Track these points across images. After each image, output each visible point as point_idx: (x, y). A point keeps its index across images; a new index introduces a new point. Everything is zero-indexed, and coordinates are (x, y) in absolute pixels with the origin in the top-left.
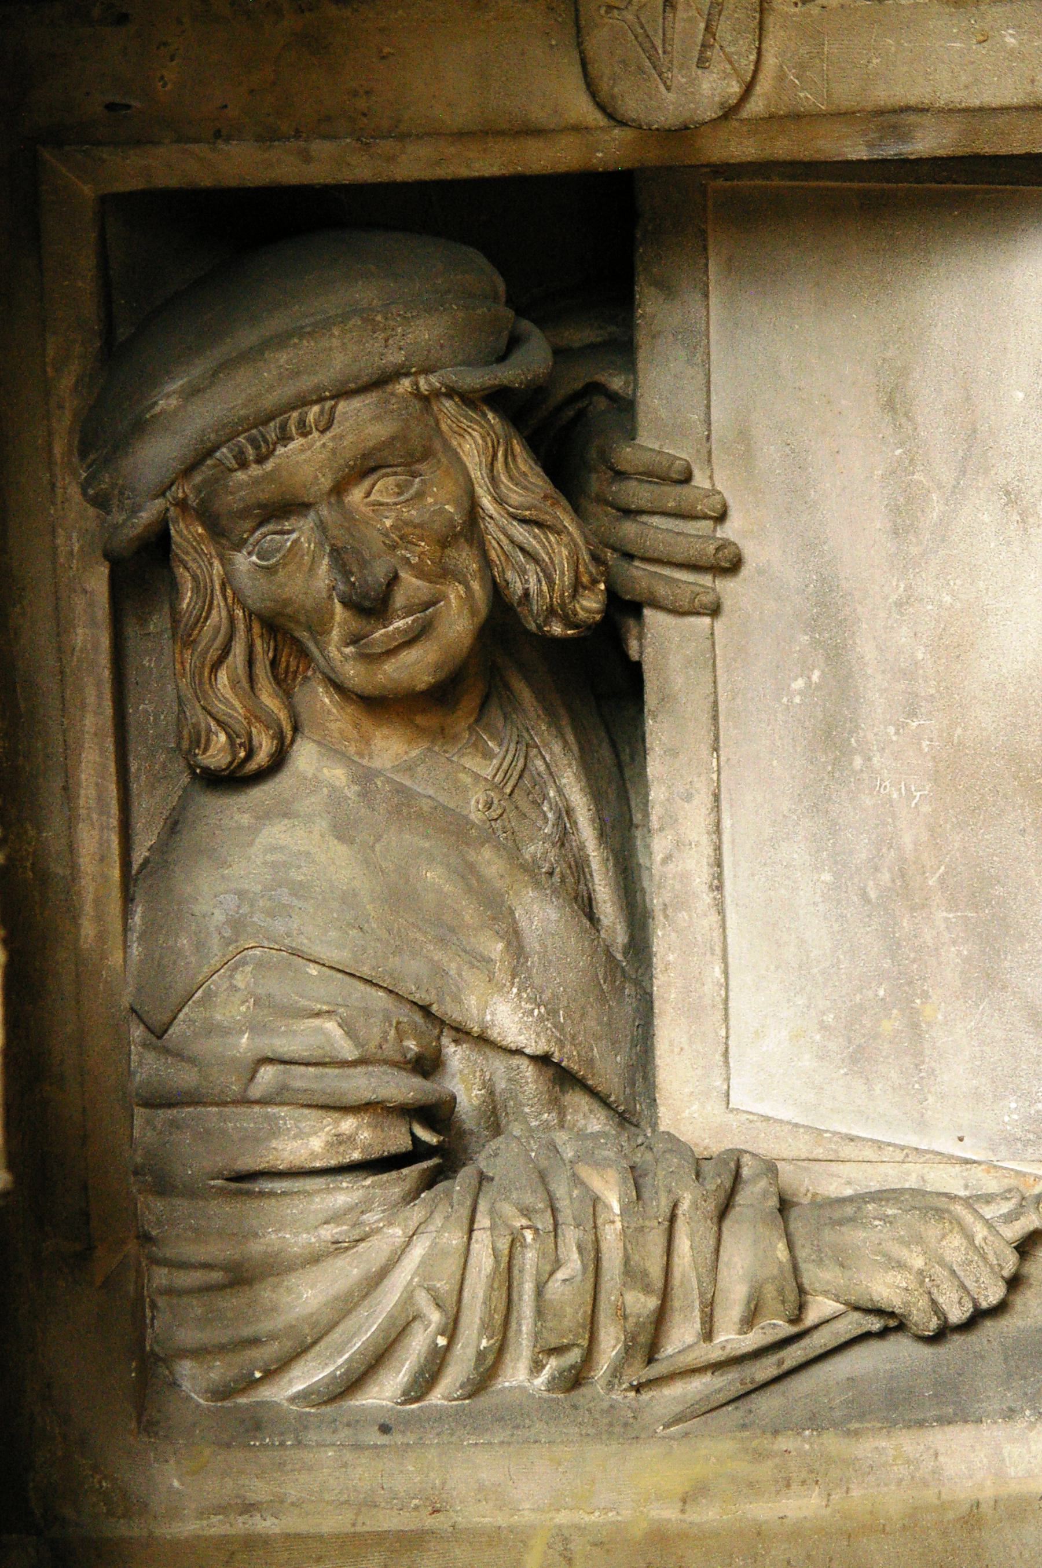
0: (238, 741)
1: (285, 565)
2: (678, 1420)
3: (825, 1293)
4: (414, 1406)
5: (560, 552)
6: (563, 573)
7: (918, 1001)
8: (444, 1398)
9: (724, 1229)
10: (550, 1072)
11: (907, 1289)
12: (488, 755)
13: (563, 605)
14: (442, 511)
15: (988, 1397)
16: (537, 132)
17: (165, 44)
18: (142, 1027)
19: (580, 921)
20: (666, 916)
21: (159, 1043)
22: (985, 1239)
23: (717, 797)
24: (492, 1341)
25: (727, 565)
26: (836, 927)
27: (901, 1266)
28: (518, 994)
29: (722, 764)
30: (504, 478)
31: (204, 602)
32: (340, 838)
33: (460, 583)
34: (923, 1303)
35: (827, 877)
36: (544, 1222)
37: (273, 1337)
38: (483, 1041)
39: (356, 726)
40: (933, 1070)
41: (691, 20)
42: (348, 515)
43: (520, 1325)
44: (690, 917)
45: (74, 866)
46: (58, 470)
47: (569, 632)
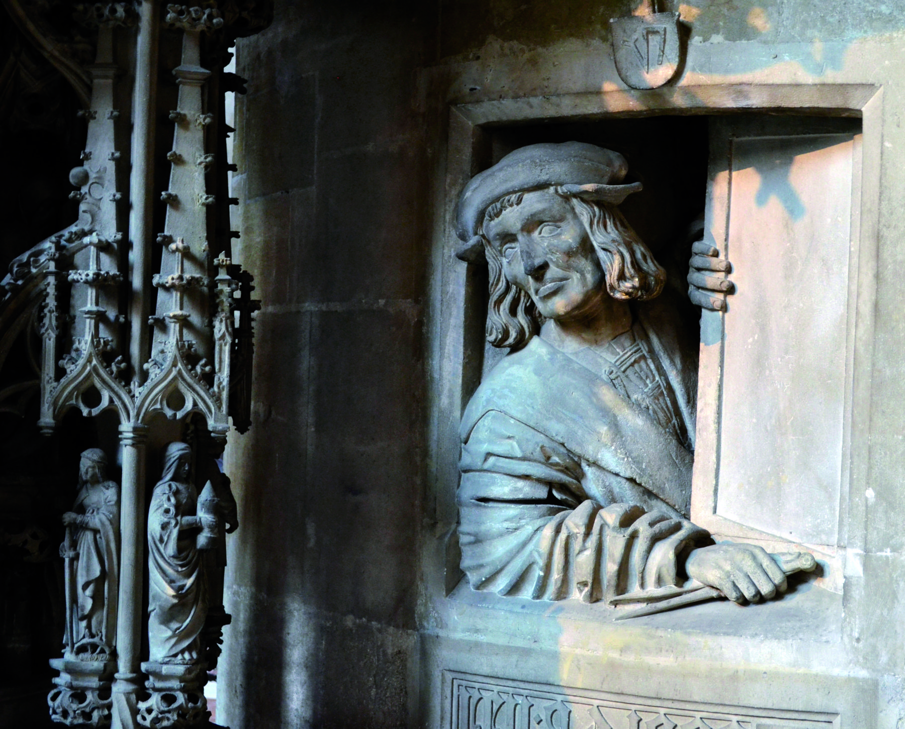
1: (513, 261)
17: (489, 66)
32: (536, 374)
33: (577, 272)
39: (559, 335)
46: (447, 225)
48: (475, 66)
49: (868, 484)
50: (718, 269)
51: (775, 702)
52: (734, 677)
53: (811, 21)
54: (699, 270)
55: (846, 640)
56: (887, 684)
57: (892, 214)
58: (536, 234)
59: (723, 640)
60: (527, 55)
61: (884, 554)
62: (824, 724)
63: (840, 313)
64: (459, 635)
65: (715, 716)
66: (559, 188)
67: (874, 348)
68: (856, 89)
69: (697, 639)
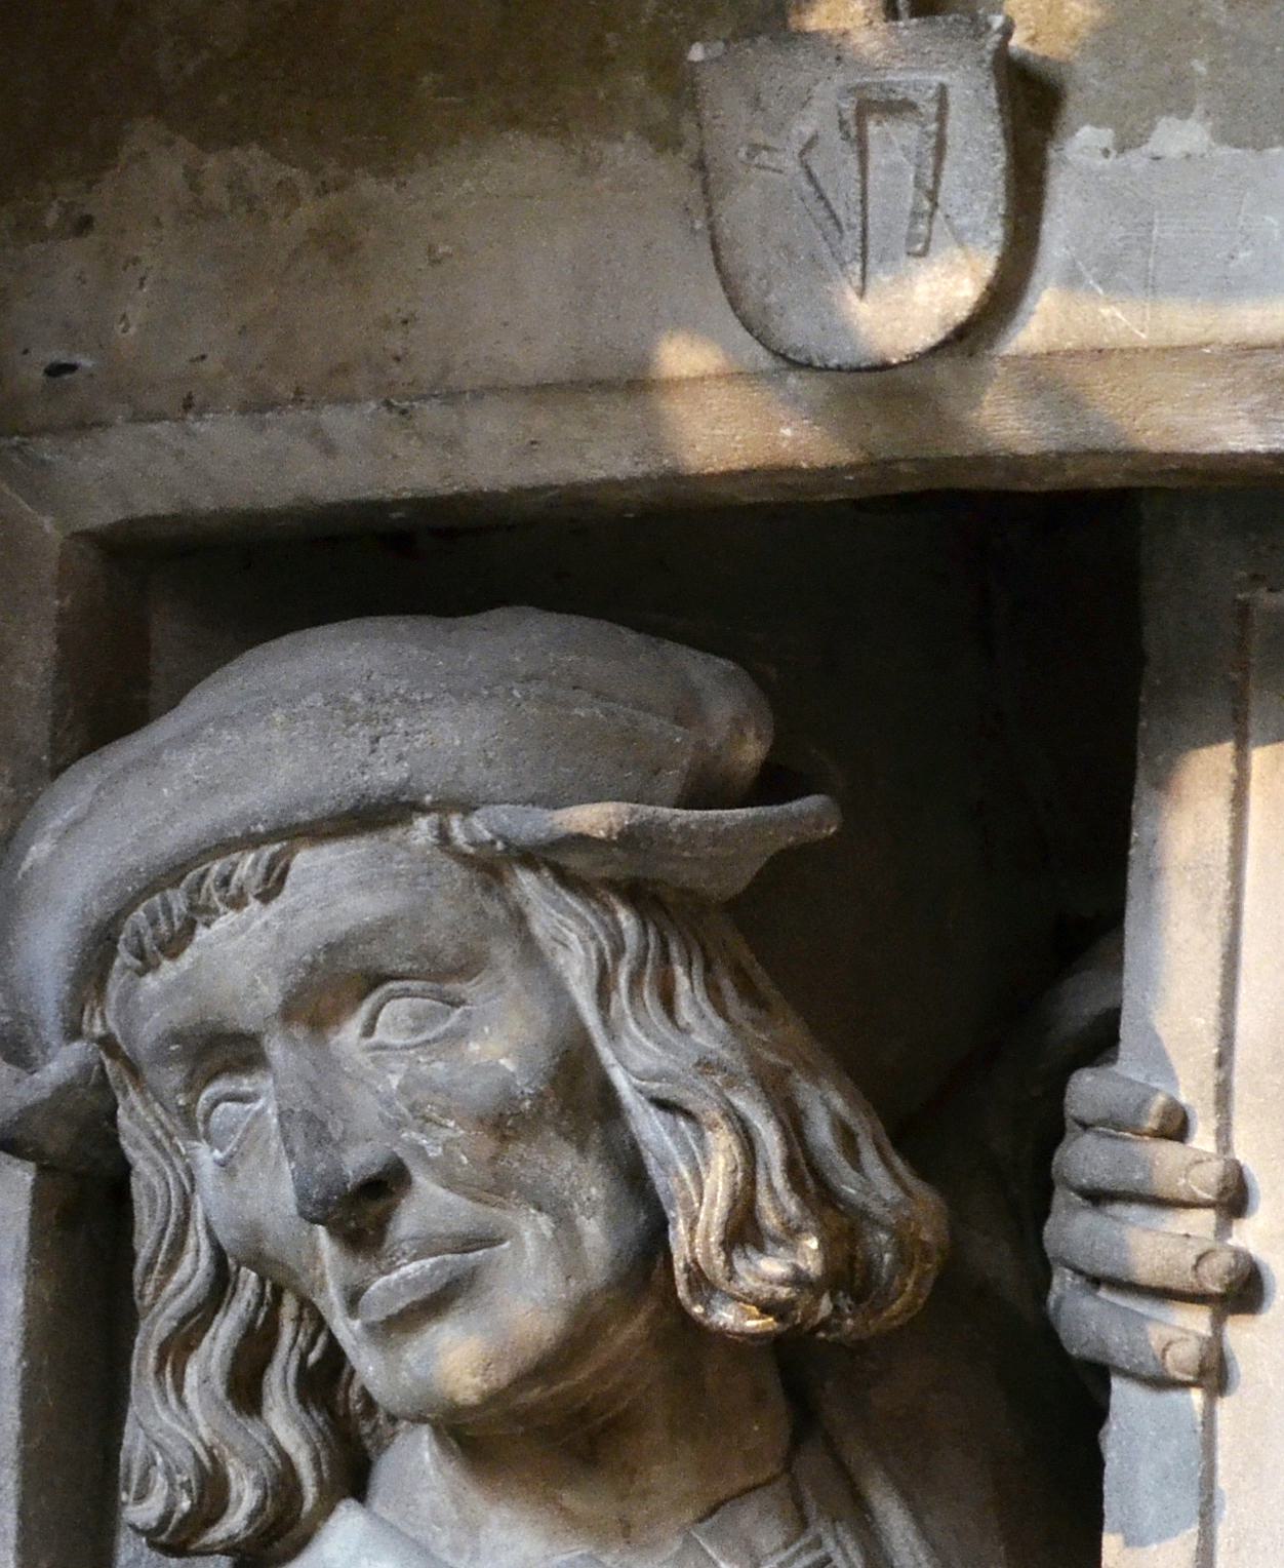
17: (136, 261)
33: (540, 1209)
39: (456, 1500)
48: (73, 259)
50: (1185, 1197)
54: (1097, 1197)
58: (349, 1034)
60: (309, 212)
66: (455, 824)
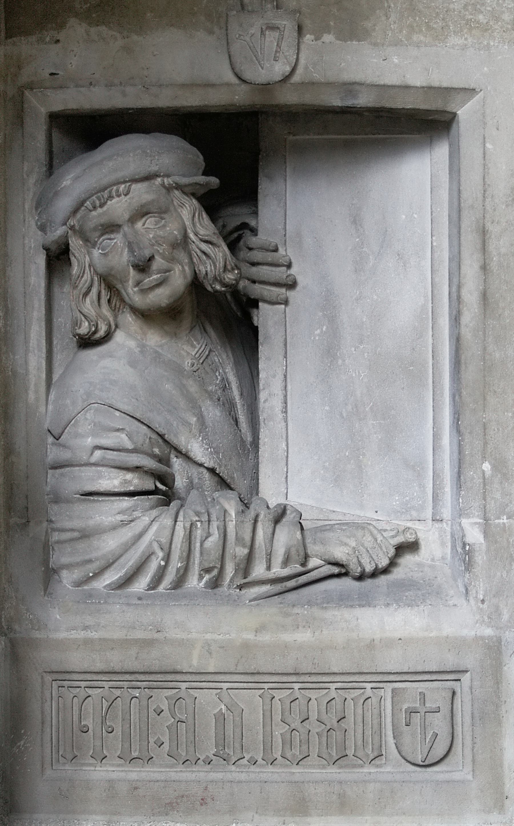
0: (92, 323)
1: (111, 252)
2: (255, 599)
3: (316, 556)
4: (152, 592)
5: (219, 255)
6: (220, 263)
7: (361, 457)
8: (164, 589)
9: (277, 530)
10: (216, 479)
11: (348, 554)
12: (193, 346)
13: (219, 275)
14: (173, 233)
15: (380, 600)
16: (213, 85)
17: (73, 51)
18: (52, 437)
19: (229, 420)
20: (265, 424)
21: (58, 442)
22: (381, 541)
23: (285, 376)
24: (182, 564)
25: (291, 283)
26: (330, 428)
27: (346, 544)
28: (202, 440)
29: (288, 364)
30: (198, 225)
31: (81, 270)
32: (131, 366)
34: (355, 560)
35: (327, 408)
36: (205, 518)
37: (97, 559)
38: (187, 457)
39: (141, 329)
40: (366, 484)
41: (271, 41)
42: (136, 232)
43: (194, 560)
44: (274, 424)
45: (27, 370)
46: (26, 214)
47: (223, 289)
49: (484, 458)
51: (411, 666)
52: (371, 645)
53: (417, 26)
55: (472, 602)
56: (509, 640)
57: (495, 210)
59: (358, 612)
60: (120, 42)
61: (501, 521)
62: (451, 682)
63: (420, 303)
64: (62, 635)
65: (350, 685)
66: (166, 180)
67: (484, 333)
68: (459, 93)
69: (334, 613)
